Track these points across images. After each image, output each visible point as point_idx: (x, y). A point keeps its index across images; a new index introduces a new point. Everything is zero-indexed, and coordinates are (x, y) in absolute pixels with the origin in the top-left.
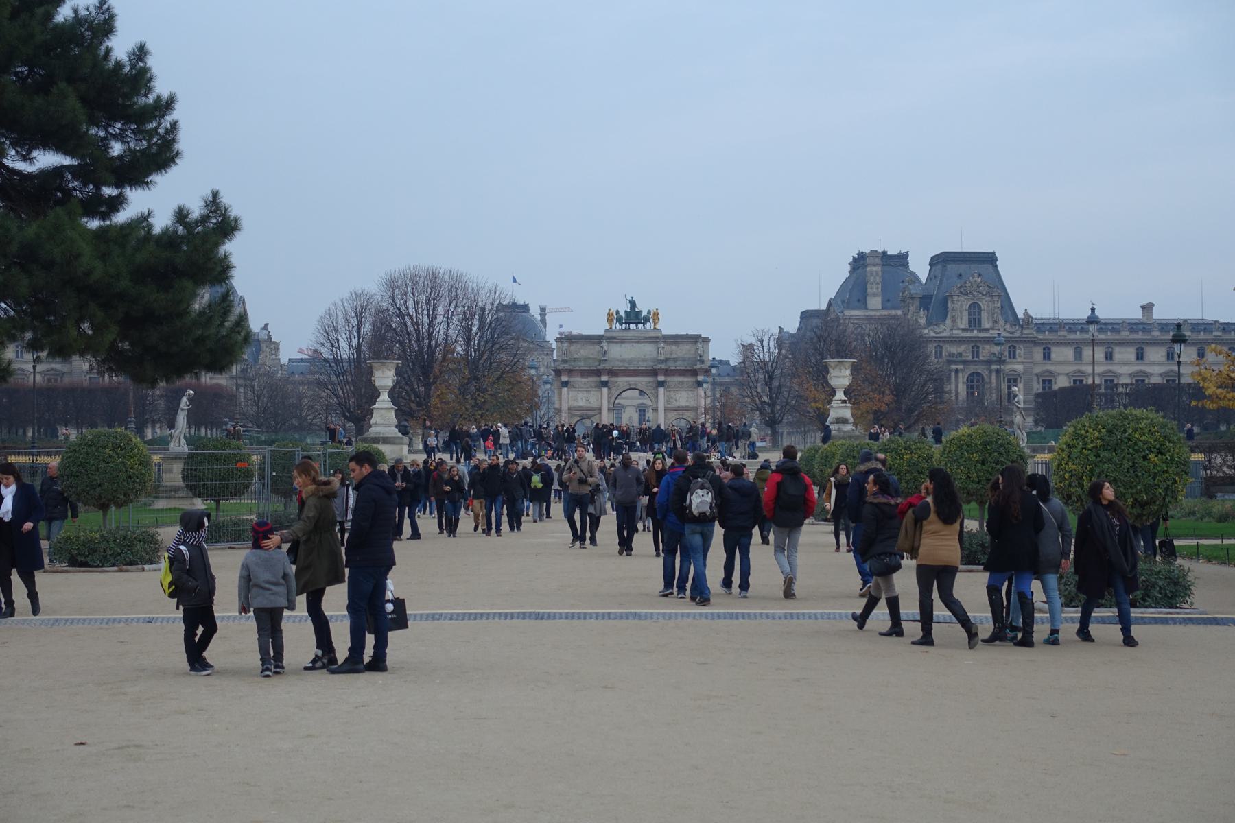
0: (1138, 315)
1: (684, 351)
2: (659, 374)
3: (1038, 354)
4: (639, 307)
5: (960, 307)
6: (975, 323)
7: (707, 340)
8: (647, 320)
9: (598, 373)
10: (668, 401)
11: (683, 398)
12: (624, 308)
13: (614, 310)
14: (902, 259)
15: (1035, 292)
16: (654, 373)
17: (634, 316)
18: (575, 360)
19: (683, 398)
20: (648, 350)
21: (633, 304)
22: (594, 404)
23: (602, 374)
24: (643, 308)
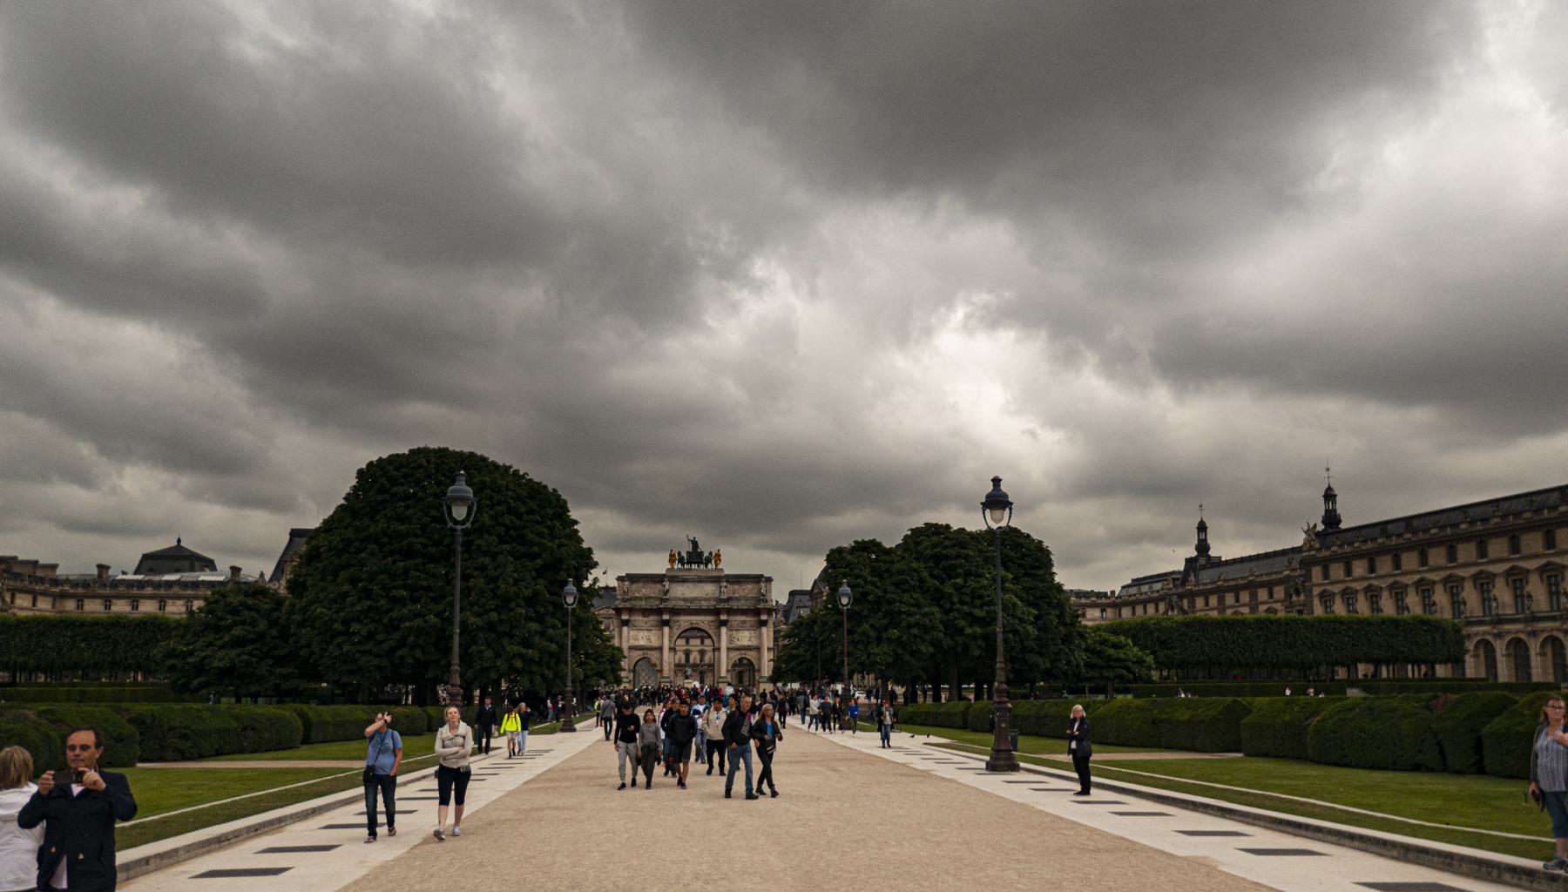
2: (721, 612)
4: (701, 548)
7: (769, 580)
9: (659, 612)
10: (730, 640)
11: (745, 638)
12: (686, 549)
16: (716, 612)
17: (695, 556)
19: (745, 638)
20: (709, 590)
22: (655, 643)
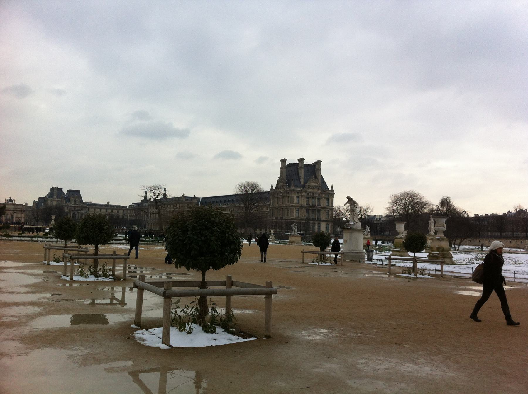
5: (72, 200)
11: (19, 215)
15: (86, 198)
16: (14, 211)
20: (13, 206)
24: (12, 199)
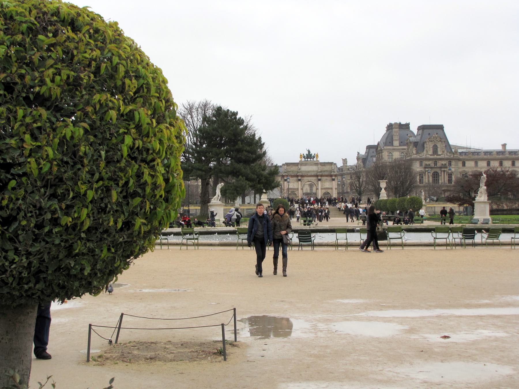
0: (500, 148)
1: (327, 168)
2: (319, 176)
3: (460, 164)
4: (311, 152)
6: (435, 152)
8: (314, 157)
9: (297, 176)
10: (322, 186)
11: (327, 185)
12: (306, 153)
13: (302, 154)
14: (407, 126)
16: (317, 176)
17: (309, 156)
18: (289, 171)
19: (327, 185)
21: (309, 152)
22: (296, 187)
23: (299, 177)
24: (313, 153)
